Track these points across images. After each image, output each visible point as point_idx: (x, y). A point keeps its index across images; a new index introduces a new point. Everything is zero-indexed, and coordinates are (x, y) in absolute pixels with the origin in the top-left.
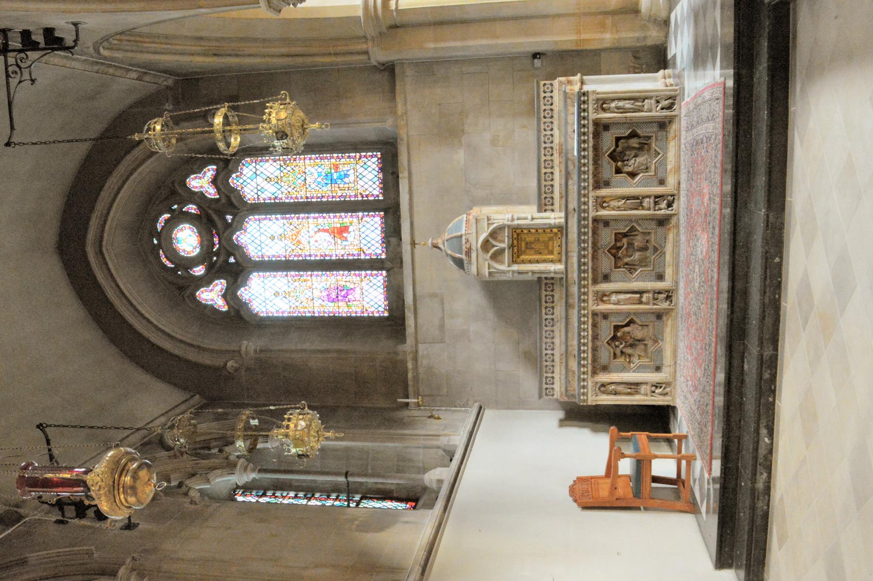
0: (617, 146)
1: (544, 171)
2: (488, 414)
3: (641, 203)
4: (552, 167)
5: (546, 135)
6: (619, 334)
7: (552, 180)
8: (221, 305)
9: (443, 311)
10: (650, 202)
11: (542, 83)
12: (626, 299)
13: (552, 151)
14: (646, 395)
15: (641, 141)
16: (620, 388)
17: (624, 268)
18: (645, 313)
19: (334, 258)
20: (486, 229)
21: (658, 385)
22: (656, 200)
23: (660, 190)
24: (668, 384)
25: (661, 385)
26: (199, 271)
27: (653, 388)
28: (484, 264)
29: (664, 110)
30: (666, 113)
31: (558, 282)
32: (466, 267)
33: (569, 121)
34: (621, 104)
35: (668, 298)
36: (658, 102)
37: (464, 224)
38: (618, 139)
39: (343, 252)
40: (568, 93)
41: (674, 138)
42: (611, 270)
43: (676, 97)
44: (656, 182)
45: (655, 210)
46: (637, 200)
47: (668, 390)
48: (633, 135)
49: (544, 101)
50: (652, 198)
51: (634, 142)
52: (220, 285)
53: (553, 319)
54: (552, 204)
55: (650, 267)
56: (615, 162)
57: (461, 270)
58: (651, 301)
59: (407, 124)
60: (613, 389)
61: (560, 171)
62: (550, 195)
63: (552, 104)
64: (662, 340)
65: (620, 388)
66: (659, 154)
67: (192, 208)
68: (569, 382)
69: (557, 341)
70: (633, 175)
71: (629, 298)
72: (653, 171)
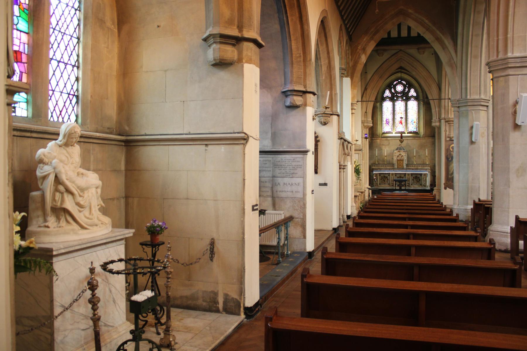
8: (385, 95)
18: (390, 182)
19: (395, 121)
23: (410, 184)
26: (393, 91)
30: (423, 185)
34: (425, 178)
35: (392, 186)
36: (425, 184)
39: (397, 123)
44: (412, 183)
48: (420, 180)
51: (418, 180)
52: (390, 95)
59: (423, 139)
67: (407, 90)
69: (382, 167)
70: (413, 180)
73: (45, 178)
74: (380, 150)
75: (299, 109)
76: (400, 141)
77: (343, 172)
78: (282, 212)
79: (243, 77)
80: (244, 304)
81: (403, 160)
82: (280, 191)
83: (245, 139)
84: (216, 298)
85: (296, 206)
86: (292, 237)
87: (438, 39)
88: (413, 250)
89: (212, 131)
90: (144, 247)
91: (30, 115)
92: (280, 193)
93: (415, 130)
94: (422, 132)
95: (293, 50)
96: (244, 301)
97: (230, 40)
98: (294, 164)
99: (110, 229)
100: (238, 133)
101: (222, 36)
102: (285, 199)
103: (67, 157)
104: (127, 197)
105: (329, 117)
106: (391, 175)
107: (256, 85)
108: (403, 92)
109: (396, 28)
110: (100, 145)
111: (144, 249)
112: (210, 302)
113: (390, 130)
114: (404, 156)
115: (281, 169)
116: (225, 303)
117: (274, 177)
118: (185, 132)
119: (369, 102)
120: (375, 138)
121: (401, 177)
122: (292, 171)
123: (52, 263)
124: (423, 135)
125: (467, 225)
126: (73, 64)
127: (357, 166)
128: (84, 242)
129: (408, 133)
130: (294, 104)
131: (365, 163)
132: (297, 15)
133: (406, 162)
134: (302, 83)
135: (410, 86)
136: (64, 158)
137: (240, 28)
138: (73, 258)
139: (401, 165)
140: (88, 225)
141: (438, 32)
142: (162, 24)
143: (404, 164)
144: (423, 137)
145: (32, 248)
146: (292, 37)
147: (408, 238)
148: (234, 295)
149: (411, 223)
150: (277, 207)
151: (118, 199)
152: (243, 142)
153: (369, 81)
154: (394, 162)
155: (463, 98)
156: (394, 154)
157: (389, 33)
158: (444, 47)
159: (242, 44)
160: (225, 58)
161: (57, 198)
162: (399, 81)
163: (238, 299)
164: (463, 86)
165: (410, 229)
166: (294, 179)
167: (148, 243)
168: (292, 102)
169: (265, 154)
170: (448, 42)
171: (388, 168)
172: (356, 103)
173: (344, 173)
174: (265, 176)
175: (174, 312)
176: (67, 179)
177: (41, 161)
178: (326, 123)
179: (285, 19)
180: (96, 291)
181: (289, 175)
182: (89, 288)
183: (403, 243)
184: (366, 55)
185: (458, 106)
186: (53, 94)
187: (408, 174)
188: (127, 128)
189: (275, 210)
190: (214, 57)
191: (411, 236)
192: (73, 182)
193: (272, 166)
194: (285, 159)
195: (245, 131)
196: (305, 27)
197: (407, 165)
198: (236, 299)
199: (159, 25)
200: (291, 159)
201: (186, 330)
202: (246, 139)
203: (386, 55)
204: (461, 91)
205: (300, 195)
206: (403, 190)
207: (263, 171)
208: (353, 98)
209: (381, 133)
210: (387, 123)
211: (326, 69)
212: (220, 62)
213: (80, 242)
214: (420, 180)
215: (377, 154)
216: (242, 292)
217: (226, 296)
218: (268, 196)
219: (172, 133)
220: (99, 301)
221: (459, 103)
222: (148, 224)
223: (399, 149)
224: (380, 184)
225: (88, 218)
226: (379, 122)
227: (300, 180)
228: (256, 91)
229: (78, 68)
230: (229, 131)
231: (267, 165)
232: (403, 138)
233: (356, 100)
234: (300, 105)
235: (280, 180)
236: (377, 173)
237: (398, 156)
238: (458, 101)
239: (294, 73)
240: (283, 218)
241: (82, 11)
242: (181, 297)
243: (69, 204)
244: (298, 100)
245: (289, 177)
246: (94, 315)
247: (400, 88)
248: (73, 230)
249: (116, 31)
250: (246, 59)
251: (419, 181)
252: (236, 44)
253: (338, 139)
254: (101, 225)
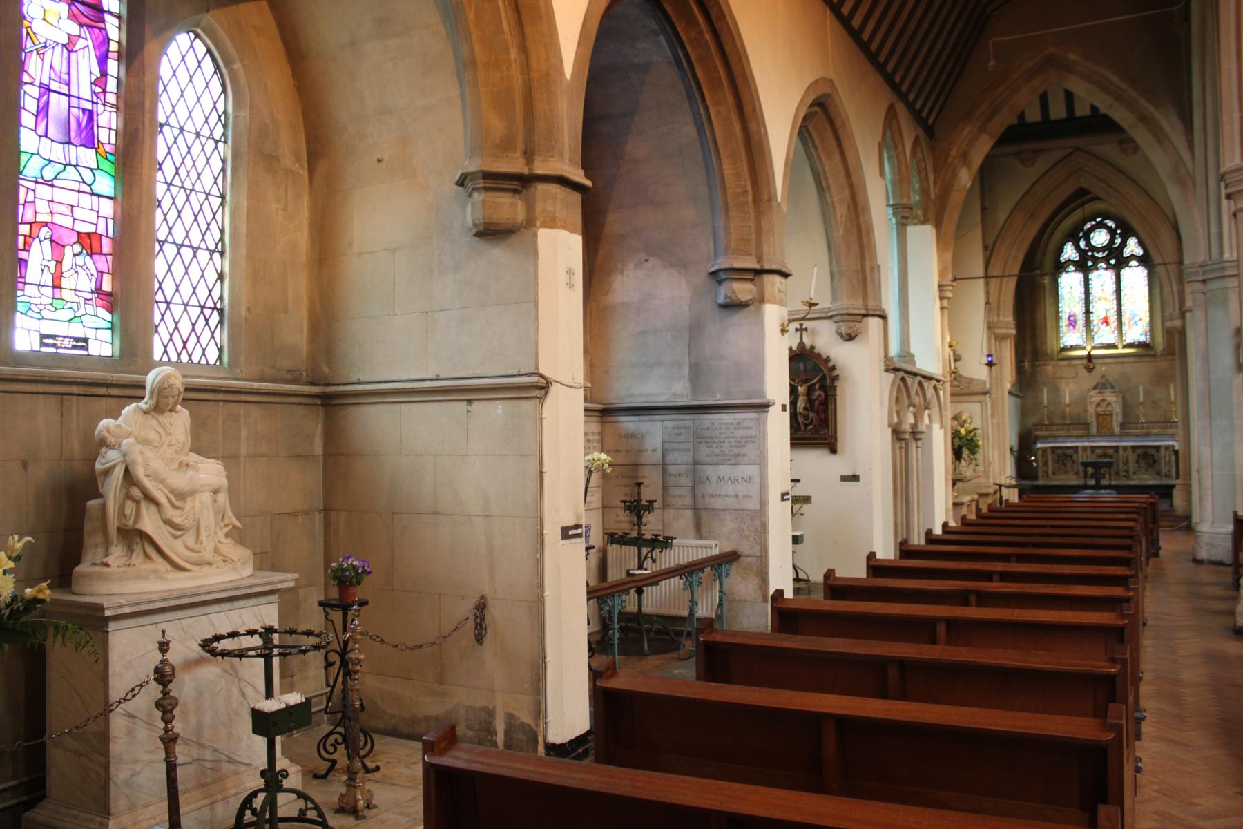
2: (1019, 400)
8: (1064, 257)
26: (1082, 244)
36: (1169, 471)
46: (1126, 463)
48: (1155, 462)
51: (1151, 462)
70: (1137, 462)
73: (107, 472)
74: (1055, 389)
75: (746, 310)
76: (1085, 367)
77: (917, 447)
78: (713, 543)
79: (537, 258)
80: (545, 738)
81: (1111, 415)
82: (711, 496)
83: (542, 388)
84: (491, 723)
85: (746, 529)
86: (737, 598)
87: (1144, 119)
88: (941, 629)
89: (479, 372)
90: (328, 609)
91: (117, 354)
92: (712, 499)
93: (1143, 339)
94: (1160, 343)
95: (727, 180)
96: (545, 729)
97: (507, 182)
98: (740, 433)
99: (249, 570)
100: (527, 375)
101: (487, 176)
102: (721, 512)
103: (159, 433)
104: (327, 510)
105: (860, 322)
106: (1080, 450)
107: (570, 272)
108: (1109, 247)
109: (1037, 101)
110: (263, 405)
111: (328, 614)
112: (480, 730)
113: (1080, 342)
114: (1113, 404)
115: (712, 447)
116: (508, 733)
117: (696, 463)
118: (430, 376)
119: (1005, 279)
120: (1041, 363)
121: (1105, 455)
122: (735, 451)
123: (107, 632)
124: (1163, 350)
125: (1133, 573)
126: (212, 247)
127: (970, 432)
128: (174, 594)
129: (1125, 347)
130: (735, 298)
131: (998, 423)
132: (731, 101)
133: (1120, 419)
134: (754, 252)
135: (1127, 232)
136: (152, 435)
137: (529, 155)
138: (154, 626)
139: (1105, 427)
140: (191, 563)
141: (1143, 102)
142: (386, 157)
144: (1162, 356)
145: (42, 601)
146: (721, 150)
147: (966, 603)
148: (525, 718)
149: (999, 567)
150: (704, 530)
151: (306, 513)
152: (537, 393)
153: (1003, 227)
154: (1090, 419)
155: (1213, 258)
156: (1088, 400)
157: (1022, 116)
158: (1160, 136)
159: (533, 188)
160: (494, 221)
161: (127, 512)
162: (1098, 220)
163: (534, 726)
164: (1214, 231)
165: (997, 581)
166: (741, 467)
167: (332, 602)
168: (729, 295)
169: (676, 412)
170: (1170, 124)
171: (1075, 433)
172: (949, 283)
173: (920, 449)
174: (678, 462)
175: (381, 742)
176: (147, 476)
177: (103, 443)
178: (853, 335)
179: (702, 112)
180: (170, 686)
181: (730, 460)
182: (155, 679)
183: (917, 614)
184: (969, 169)
185: (1201, 278)
186: (168, 308)
187: (1125, 448)
188: (326, 369)
189: (700, 537)
190: (473, 220)
191: (973, 599)
192: (162, 482)
193: (692, 439)
194: (720, 424)
195: (542, 371)
196: (753, 126)
197: (1123, 425)
198: (528, 725)
199: (380, 158)
200: (733, 424)
201: (409, 784)
202: (542, 387)
203: (1042, 164)
204: (1207, 243)
205: (753, 504)
206: (1105, 487)
207: (674, 450)
208: (942, 274)
209: (1056, 349)
210: (1072, 323)
211: (845, 211)
212: (485, 229)
213: (165, 595)
214: (1155, 462)
215: (1045, 402)
216: (539, 710)
217: (510, 717)
218: (684, 507)
219: (405, 378)
220: (175, 705)
221: (1204, 272)
222: (333, 565)
223: (1100, 387)
224: (1053, 473)
225: (192, 550)
226: (1050, 323)
227: (752, 470)
228: (570, 285)
229: (222, 254)
230: (510, 372)
231: (682, 438)
232: (1094, 361)
233: (950, 277)
234: (747, 301)
235: (709, 471)
236: (1047, 448)
237: (1098, 405)
238: (1200, 266)
239: (732, 231)
240: (717, 552)
241: (230, 142)
242: (427, 718)
243: (149, 523)
244: (743, 290)
245: (729, 462)
246: (167, 730)
247: (1100, 238)
248: (155, 572)
249: (306, 173)
250: (542, 219)
252: (520, 188)
253: (887, 370)
254: (221, 564)
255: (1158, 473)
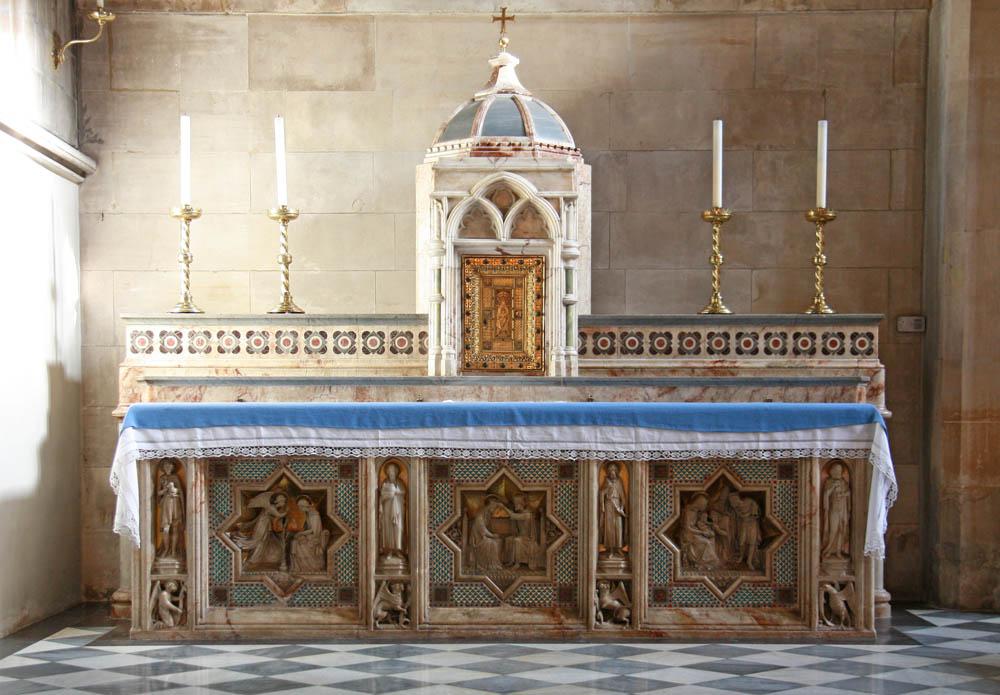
0: (744, 495)
1: (675, 332)
3: (616, 551)
4: (682, 352)
5: (756, 337)
6: (303, 503)
7: (653, 351)
9: (330, 88)
10: (618, 569)
11: (875, 331)
12: (392, 519)
13: (719, 352)
14: (155, 571)
15: (752, 549)
16: (171, 506)
17: (462, 514)
20: (547, 194)
21: (181, 594)
22: (622, 584)
23: (643, 592)
24: (183, 620)
25: (181, 605)
27: (173, 586)
28: (460, 188)
29: (823, 600)
30: (818, 606)
31: (415, 364)
32: (449, 144)
33: (791, 391)
35: (393, 615)
36: (842, 586)
37: (553, 142)
38: (759, 498)
40: (855, 388)
41: (760, 621)
42: (459, 483)
43: (853, 626)
44: (662, 581)
45: (597, 581)
46: (618, 544)
47: (170, 621)
49: (833, 335)
50: (626, 576)
51: (752, 533)
53: (324, 350)
54: (596, 352)
55: (464, 573)
56: (708, 491)
57: (439, 134)
58: (386, 576)
60: (169, 491)
61: (673, 370)
62: (618, 344)
63: (825, 352)
64: (291, 604)
65: (171, 506)
66: (723, 589)
68: (173, 389)
70: (676, 533)
71: (394, 525)
72: (682, 578)
143: (555, 321)
224: (219, 596)
251: (765, 542)
255: (787, 596)
